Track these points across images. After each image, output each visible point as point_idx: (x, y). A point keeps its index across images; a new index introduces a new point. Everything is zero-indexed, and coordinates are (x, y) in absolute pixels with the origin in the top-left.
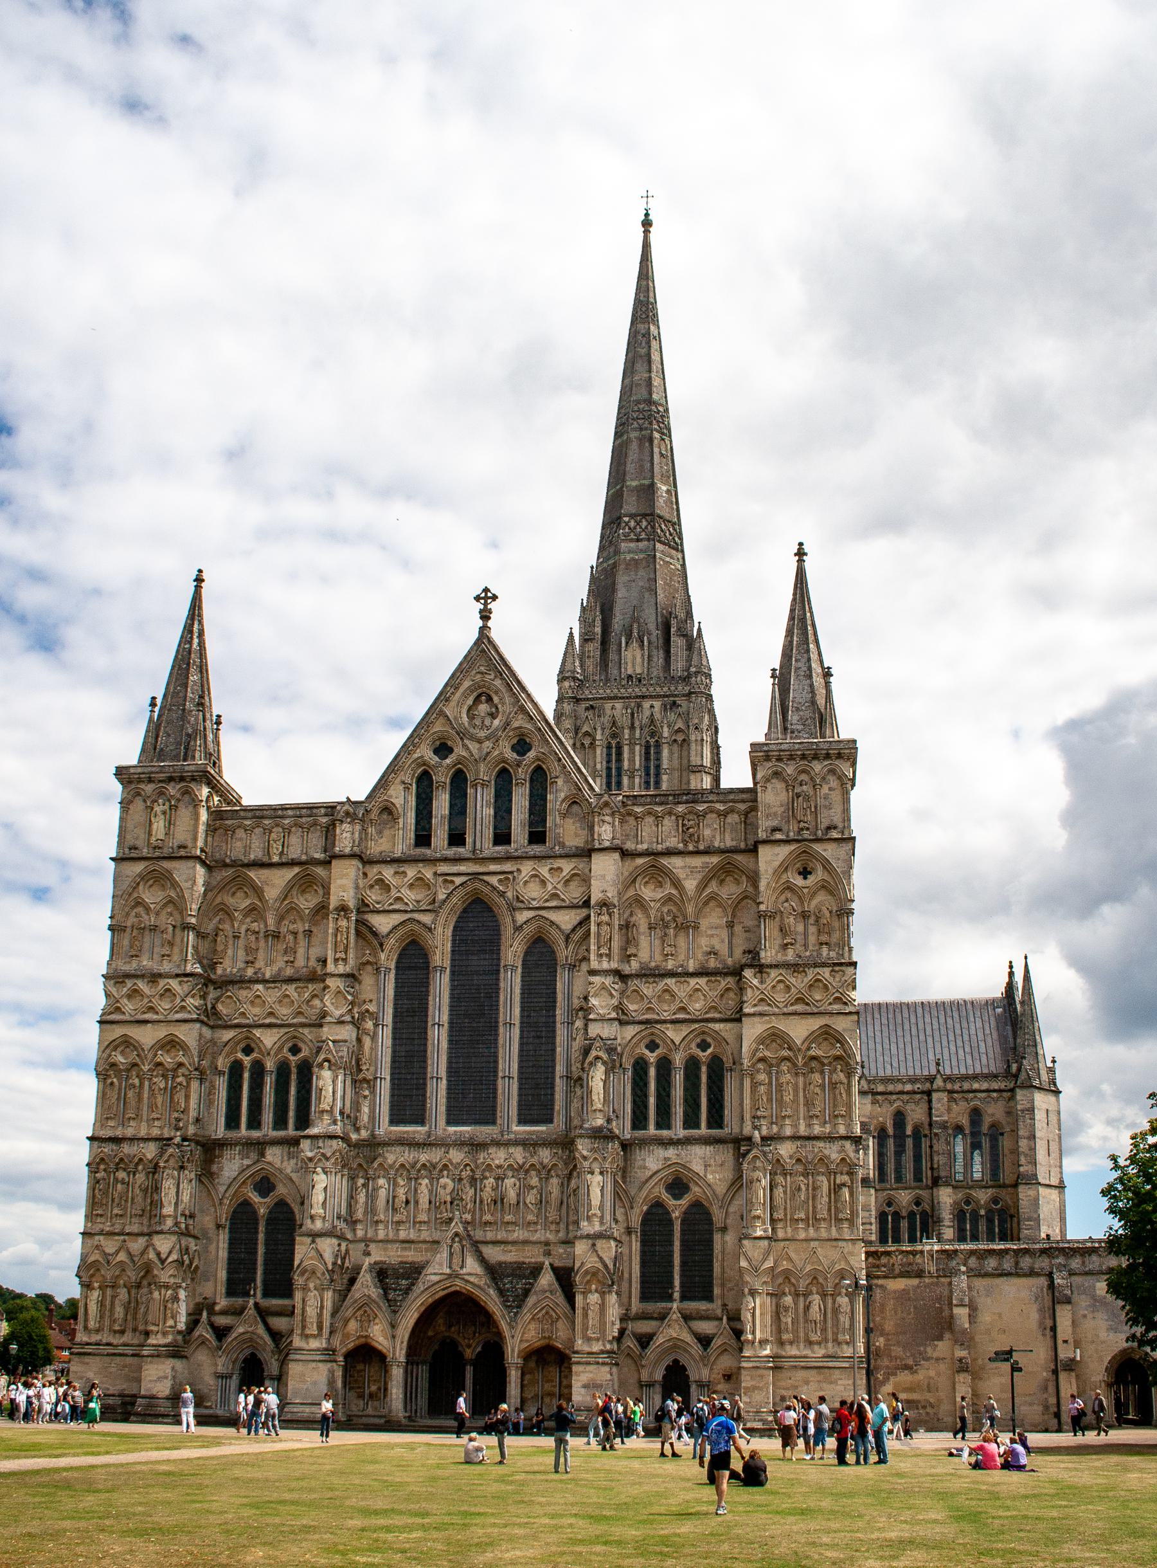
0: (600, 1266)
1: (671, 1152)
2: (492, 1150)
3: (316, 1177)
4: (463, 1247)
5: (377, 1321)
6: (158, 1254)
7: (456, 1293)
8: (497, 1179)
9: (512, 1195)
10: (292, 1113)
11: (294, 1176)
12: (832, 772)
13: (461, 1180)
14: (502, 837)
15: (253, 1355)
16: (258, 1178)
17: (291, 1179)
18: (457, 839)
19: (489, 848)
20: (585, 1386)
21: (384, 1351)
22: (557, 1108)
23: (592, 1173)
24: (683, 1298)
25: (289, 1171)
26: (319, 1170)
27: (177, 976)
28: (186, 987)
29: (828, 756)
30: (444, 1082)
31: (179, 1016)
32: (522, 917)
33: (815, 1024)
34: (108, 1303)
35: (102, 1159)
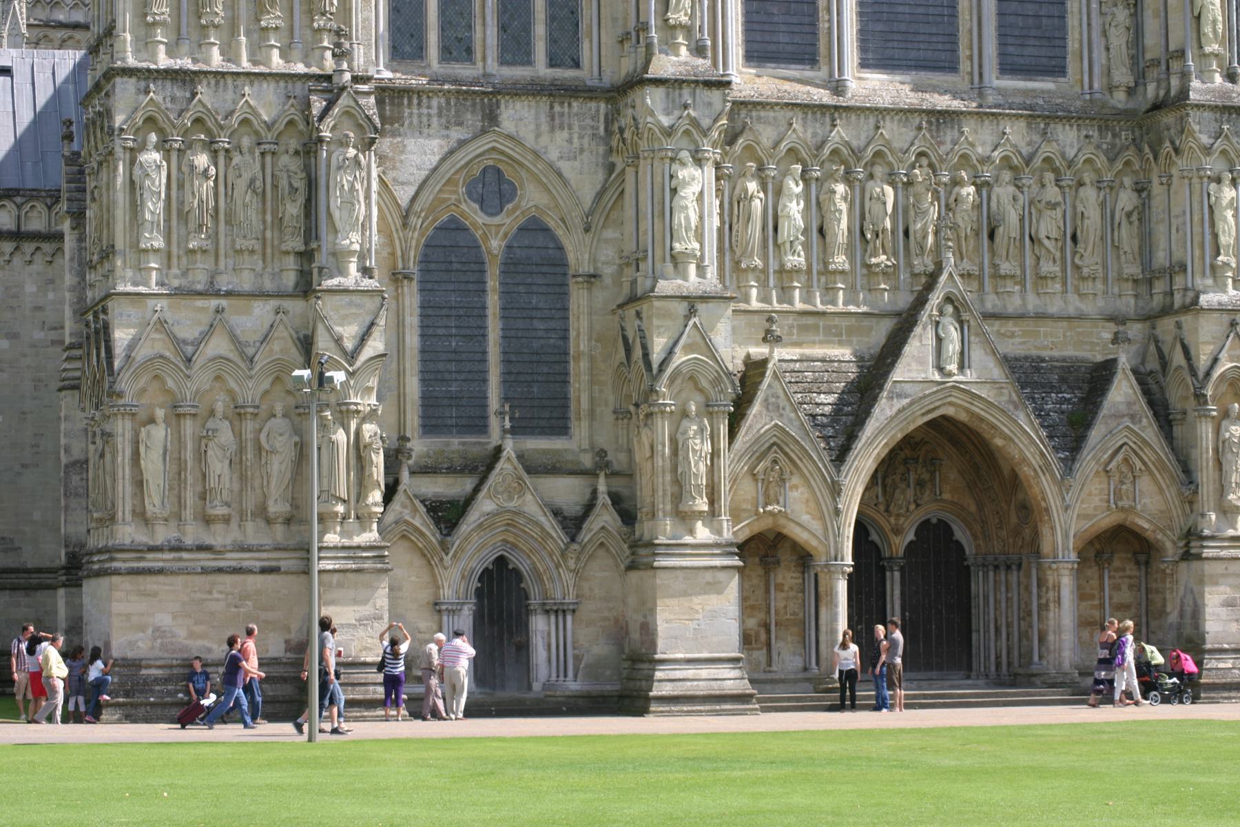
3: (683, 173)
4: (961, 323)
5: (795, 480)
6: (338, 341)
7: (943, 417)
8: (979, 188)
9: (1013, 217)
10: (540, 30)
11: (565, 167)
13: (909, 184)
15: (501, 561)
16: (477, 172)
17: (560, 175)
21: (814, 543)
22: (1072, 44)
23: (1219, 181)
25: (553, 155)
26: (685, 155)
34: (189, 455)
35: (150, 120)
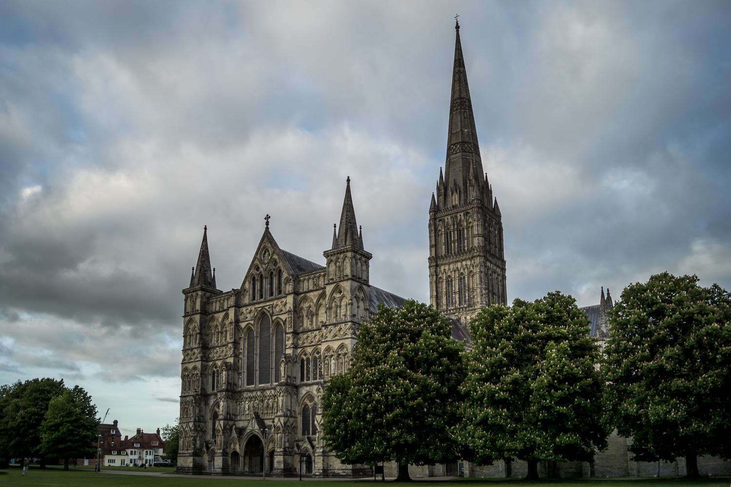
0: (280, 425)
1: (308, 388)
2: (267, 391)
12: (346, 256)
14: (272, 294)
18: (261, 297)
19: (269, 298)
20: (277, 462)
24: (313, 434)
27: (196, 348)
28: (199, 351)
29: (344, 252)
30: (258, 371)
31: (197, 360)
32: (274, 318)
33: (339, 343)
